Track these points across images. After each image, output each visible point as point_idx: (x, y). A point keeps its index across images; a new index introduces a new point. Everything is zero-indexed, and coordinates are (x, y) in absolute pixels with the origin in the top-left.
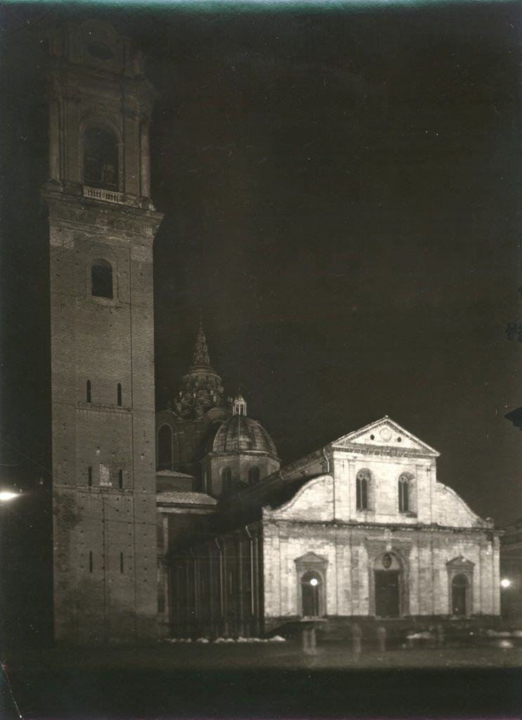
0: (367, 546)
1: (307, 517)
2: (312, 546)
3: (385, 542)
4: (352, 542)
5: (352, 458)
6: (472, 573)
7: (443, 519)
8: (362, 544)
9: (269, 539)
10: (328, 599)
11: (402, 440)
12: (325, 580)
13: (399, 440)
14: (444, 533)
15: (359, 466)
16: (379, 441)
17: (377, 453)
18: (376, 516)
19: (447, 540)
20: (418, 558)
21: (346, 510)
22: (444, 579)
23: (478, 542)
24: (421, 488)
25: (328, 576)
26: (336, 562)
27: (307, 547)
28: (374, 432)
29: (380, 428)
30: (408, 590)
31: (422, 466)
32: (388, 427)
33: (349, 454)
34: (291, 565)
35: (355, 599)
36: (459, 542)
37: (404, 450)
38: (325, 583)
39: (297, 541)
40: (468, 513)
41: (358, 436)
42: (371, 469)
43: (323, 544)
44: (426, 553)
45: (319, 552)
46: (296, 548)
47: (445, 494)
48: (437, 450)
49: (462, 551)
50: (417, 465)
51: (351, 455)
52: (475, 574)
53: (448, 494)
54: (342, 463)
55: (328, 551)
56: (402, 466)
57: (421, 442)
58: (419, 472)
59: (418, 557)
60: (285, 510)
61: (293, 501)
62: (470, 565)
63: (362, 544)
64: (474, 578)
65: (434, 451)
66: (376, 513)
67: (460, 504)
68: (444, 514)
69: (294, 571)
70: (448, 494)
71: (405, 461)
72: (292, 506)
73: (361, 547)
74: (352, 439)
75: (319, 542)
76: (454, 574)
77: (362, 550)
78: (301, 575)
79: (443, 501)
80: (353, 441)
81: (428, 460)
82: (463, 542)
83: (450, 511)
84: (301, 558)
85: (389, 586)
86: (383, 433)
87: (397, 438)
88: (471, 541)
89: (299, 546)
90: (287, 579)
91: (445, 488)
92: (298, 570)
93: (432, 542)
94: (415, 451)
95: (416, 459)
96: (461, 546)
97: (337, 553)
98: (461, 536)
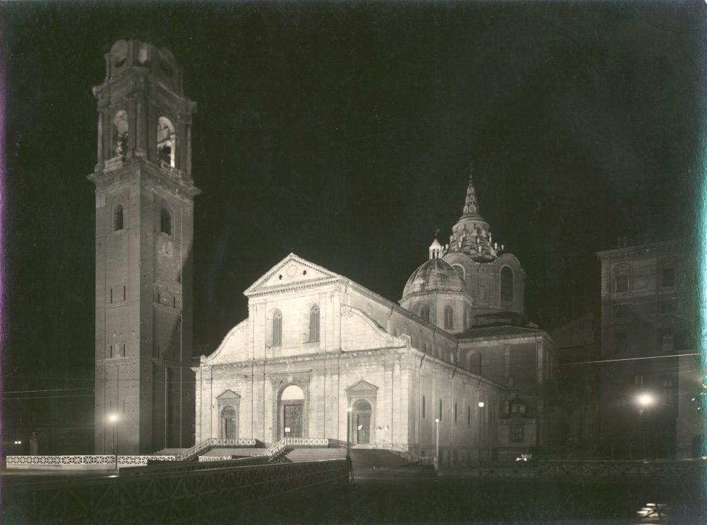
0: (271, 380)
1: (231, 360)
3: (286, 374)
5: (262, 301)
6: (375, 398)
8: (267, 378)
11: (307, 272)
12: (238, 413)
13: (305, 273)
14: (345, 358)
15: (269, 307)
17: (283, 291)
19: (347, 365)
20: (317, 387)
21: (259, 351)
23: (382, 363)
24: (324, 316)
25: (241, 409)
26: (247, 396)
27: (225, 385)
28: (281, 272)
29: (286, 267)
30: (308, 418)
32: (295, 263)
34: (215, 401)
35: (261, 429)
36: (361, 366)
37: (309, 281)
38: (238, 416)
40: (376, 332)
41: (266, 280)
42: (279, 308)
43: (237, 382)
48: (338, 273)
49: (364, 375)
50: (319, 294)
51: (261, 299)
52: (378, 399)
53: (355, 316)
54: (255, 308)
56: (306, 298)
57: (326, 271)
58: (323, 300)
61: (220, 348)
63: (267, 378)
64: (378, 401)
65: (334, 274)
66: (283, 347)
69: (216, 406)
70: (355, 316)
71: (309, 291)
73: (266, 382)
74: (262, 283)
76: (354, 400)
77: (268, 385)
78: (221, 408)
81: (333, 286)
83: (356, 334)
84: (221, 395)
85: (291, 416)
86: (292, 268)
87: (302, 272)
88: (375, 363)
91: (351, 311)
92: (219, 406)
93: (331, 369)
94: (319, 279)
95: (318, 288)
96: (363, 370)
97: (248, 389)
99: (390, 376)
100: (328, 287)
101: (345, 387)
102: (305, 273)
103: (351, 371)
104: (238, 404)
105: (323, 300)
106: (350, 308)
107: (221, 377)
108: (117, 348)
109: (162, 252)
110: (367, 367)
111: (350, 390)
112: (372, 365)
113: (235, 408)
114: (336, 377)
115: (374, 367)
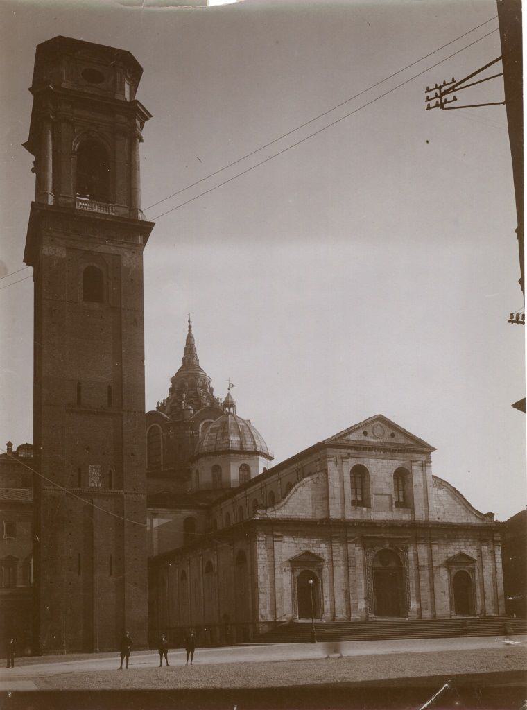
4: (345, 542)
7: (441, 513)
9: (264, 539)
13: (393, 435)
15: (353, 462)
16: (371, 437)
22: (443, 576)
24: (417, 483)
33: (343, 450)
38: (322, 584)
44: (423, 551)
45: (315, 550)
46: (288, 547)
51: (344, 452)
55: (321, 549)
72: (285, 504)
75: (314, 541)
76: (454, 572)
77: (357, 551)
78: (297, 574)
87: (390, 434)
90: (282, 579)
92: (292, 571)
95: (409, 455)
105: (414, 468)
111: (449, 563)
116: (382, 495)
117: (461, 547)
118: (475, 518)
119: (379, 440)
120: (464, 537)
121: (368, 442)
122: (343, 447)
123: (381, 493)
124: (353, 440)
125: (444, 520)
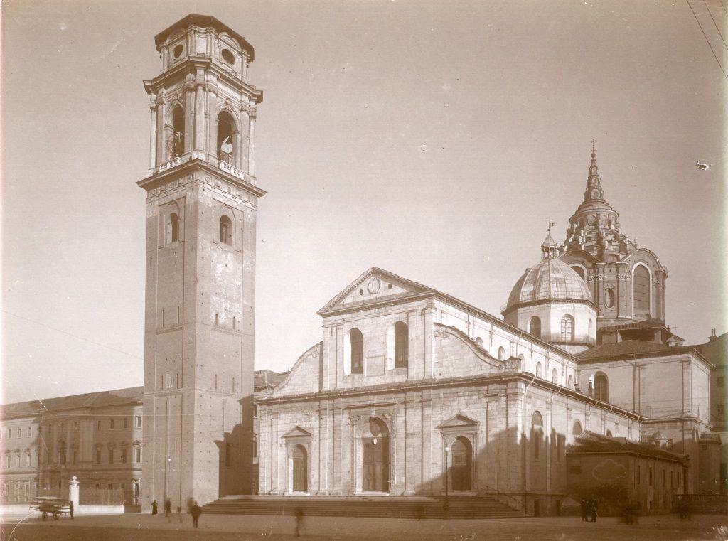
2: (299, 420)
10: (312, 473)
13: (390, 287)
16: (368, 295)
17: (364, 309)
18: (365, 380)
19: (442, 395)
25: (313, 448)
31: (414, 311)
33: (339, 317)
39: (287, 416)
44: (414, 416)
45: (305, 426)
46: (285, 422)
47: (445, 337)
49: (464, 407)
51: (338, 318)
55: (312, 423)
56: (392, 316)
59: (406, 421)
60: (283, 387)
62: (473, 423)
67: (466, 347)
68: (445, 363)
69: (284, 446)
71: (396, 308)
77: (344, 419)
79: (444, 346)
80: (342, 303)
82: (464, 396)
89: (288, 421)
92: (286, 445)
98: (460, 389)
99: (494, 409)
100: (419, 303)
101: (439, 423)
102: (390, 287)
103: (447, 403)
104: (309, 444)
106: (444, 329)
107: (287, 411)
108: (169, 378)
109: (220, 268)
110: (466, 398)
112: (472, 395)
113: (306, 446)
114: (428, 411)
115: (475, 397)
116: (375, 357)
117: (461, 407)
118: (489, 367)
119: (375, 296)
120: (467, 393)
121: (363, 301)
122: (338, 313)
123: (373, 355)
124: (348, 304)
125: (447, 376)
